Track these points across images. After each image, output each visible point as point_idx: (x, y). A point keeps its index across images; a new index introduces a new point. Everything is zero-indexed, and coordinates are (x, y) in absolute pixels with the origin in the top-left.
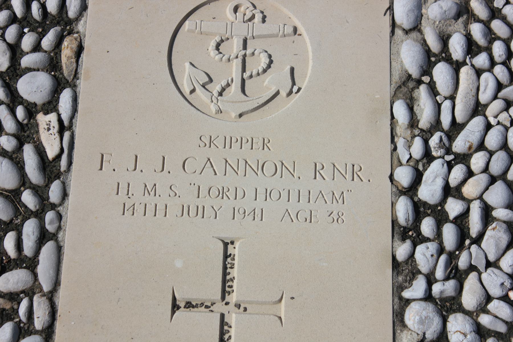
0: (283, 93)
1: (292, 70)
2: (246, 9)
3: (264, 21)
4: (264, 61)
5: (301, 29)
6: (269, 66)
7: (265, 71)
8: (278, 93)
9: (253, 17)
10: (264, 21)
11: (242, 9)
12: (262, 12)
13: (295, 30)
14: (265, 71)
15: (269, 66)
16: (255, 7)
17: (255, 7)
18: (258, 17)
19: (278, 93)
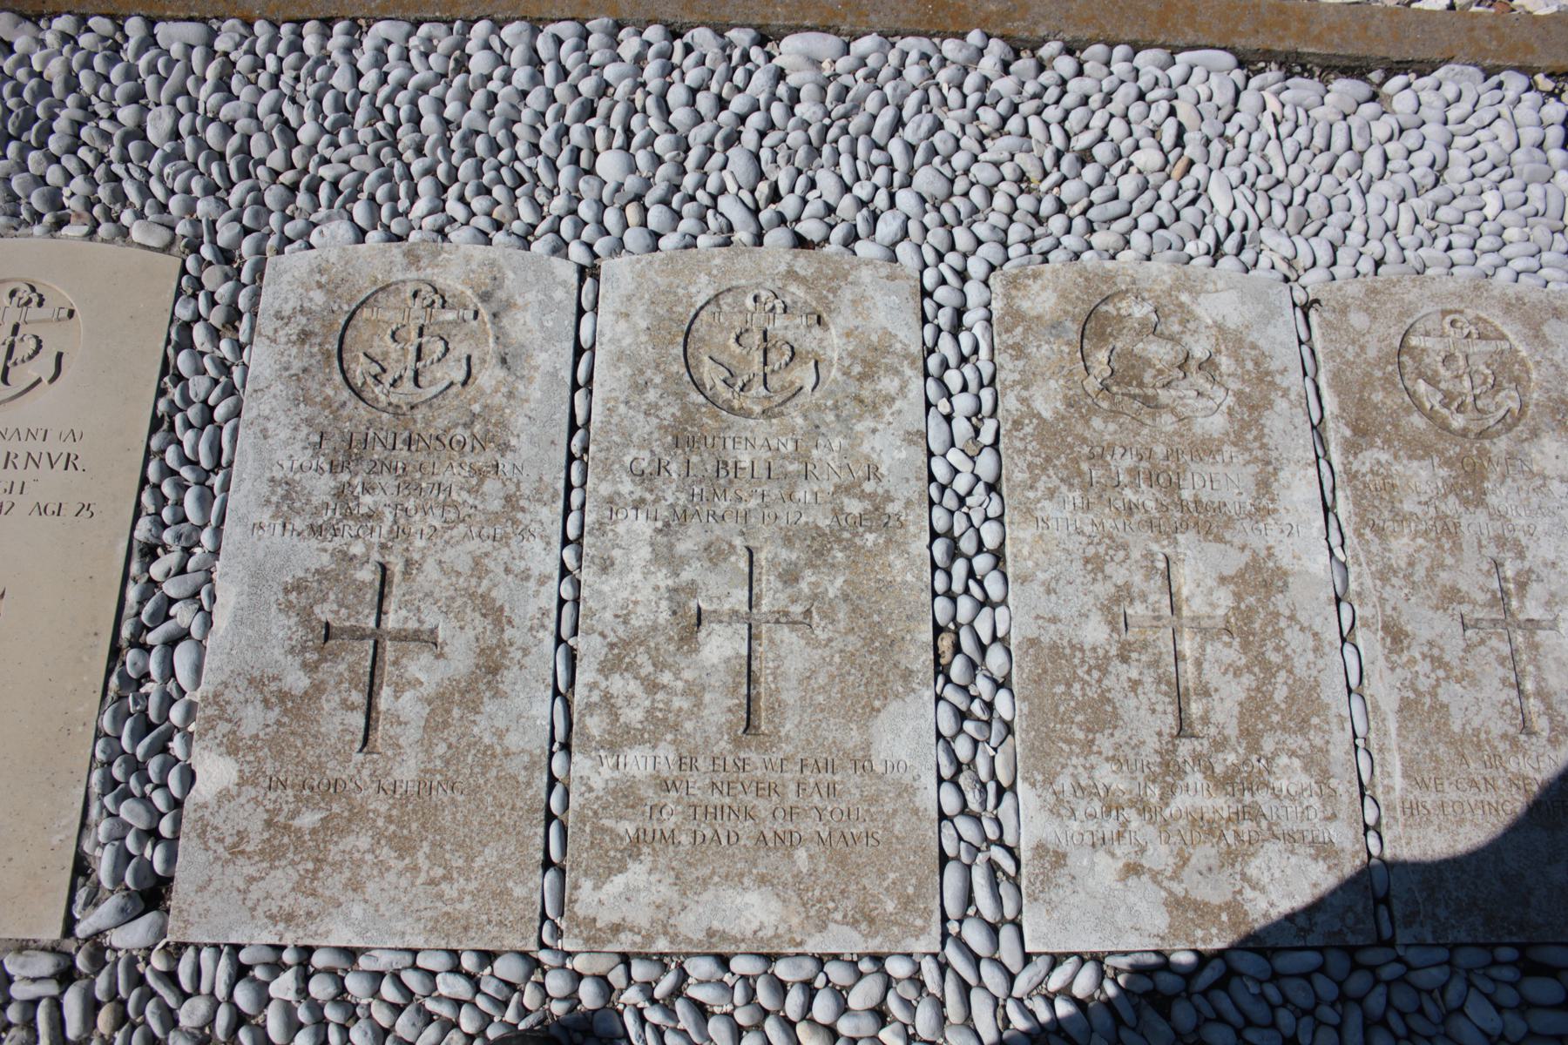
0: (45, 381)
1: (59, 356)
2: (24, 293)
3: (40, 304)
4: (32, 344)
5: (77, 312)
6: (36, 352)
7: (30, 358)
8: (39, 381)
9: (30, 301)
10: (40, 304)
11: (19, 294)
12: (40, 296)
13: (71, 314)
14: (30, 358)
15: (36, 352)
16: (33, 289)
17: (33, 289)
18: (35, 300)
19: (39, 381)
